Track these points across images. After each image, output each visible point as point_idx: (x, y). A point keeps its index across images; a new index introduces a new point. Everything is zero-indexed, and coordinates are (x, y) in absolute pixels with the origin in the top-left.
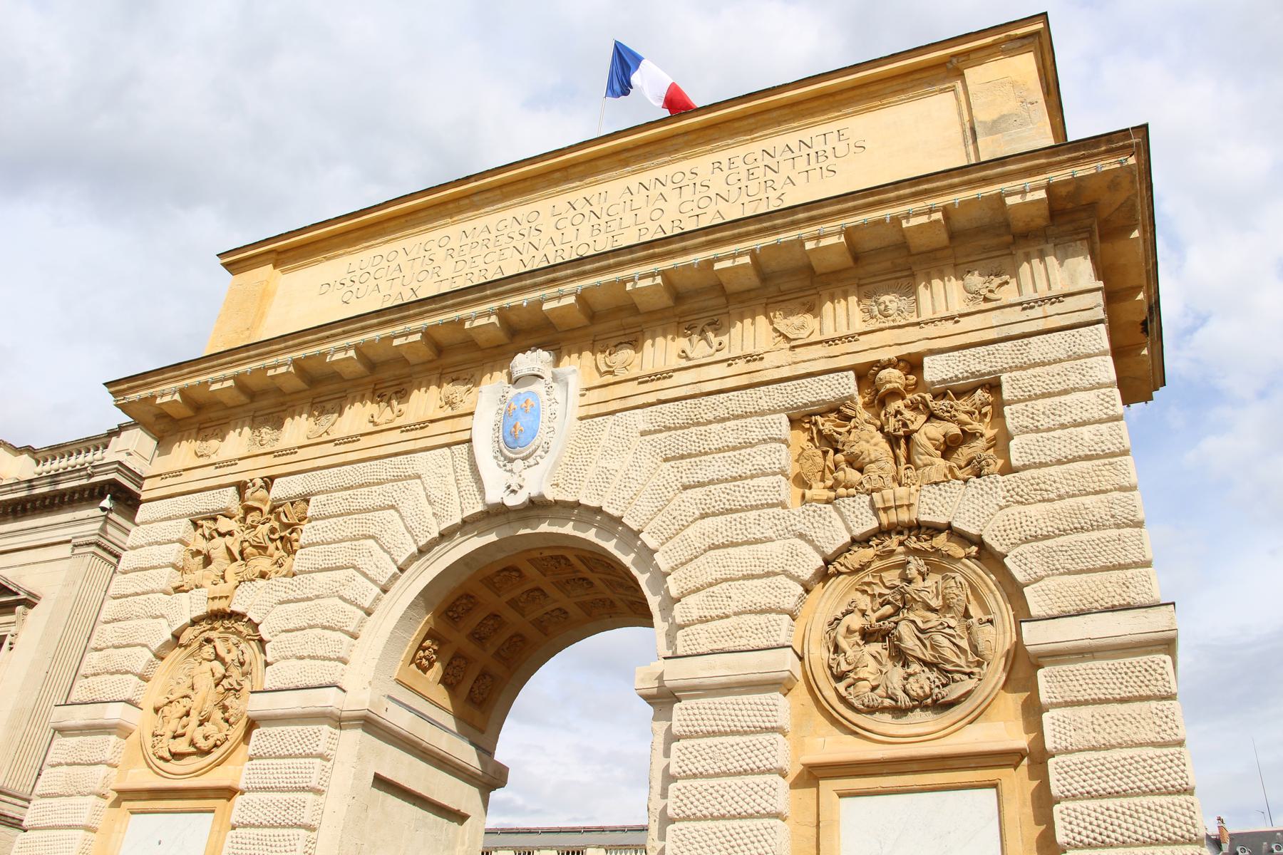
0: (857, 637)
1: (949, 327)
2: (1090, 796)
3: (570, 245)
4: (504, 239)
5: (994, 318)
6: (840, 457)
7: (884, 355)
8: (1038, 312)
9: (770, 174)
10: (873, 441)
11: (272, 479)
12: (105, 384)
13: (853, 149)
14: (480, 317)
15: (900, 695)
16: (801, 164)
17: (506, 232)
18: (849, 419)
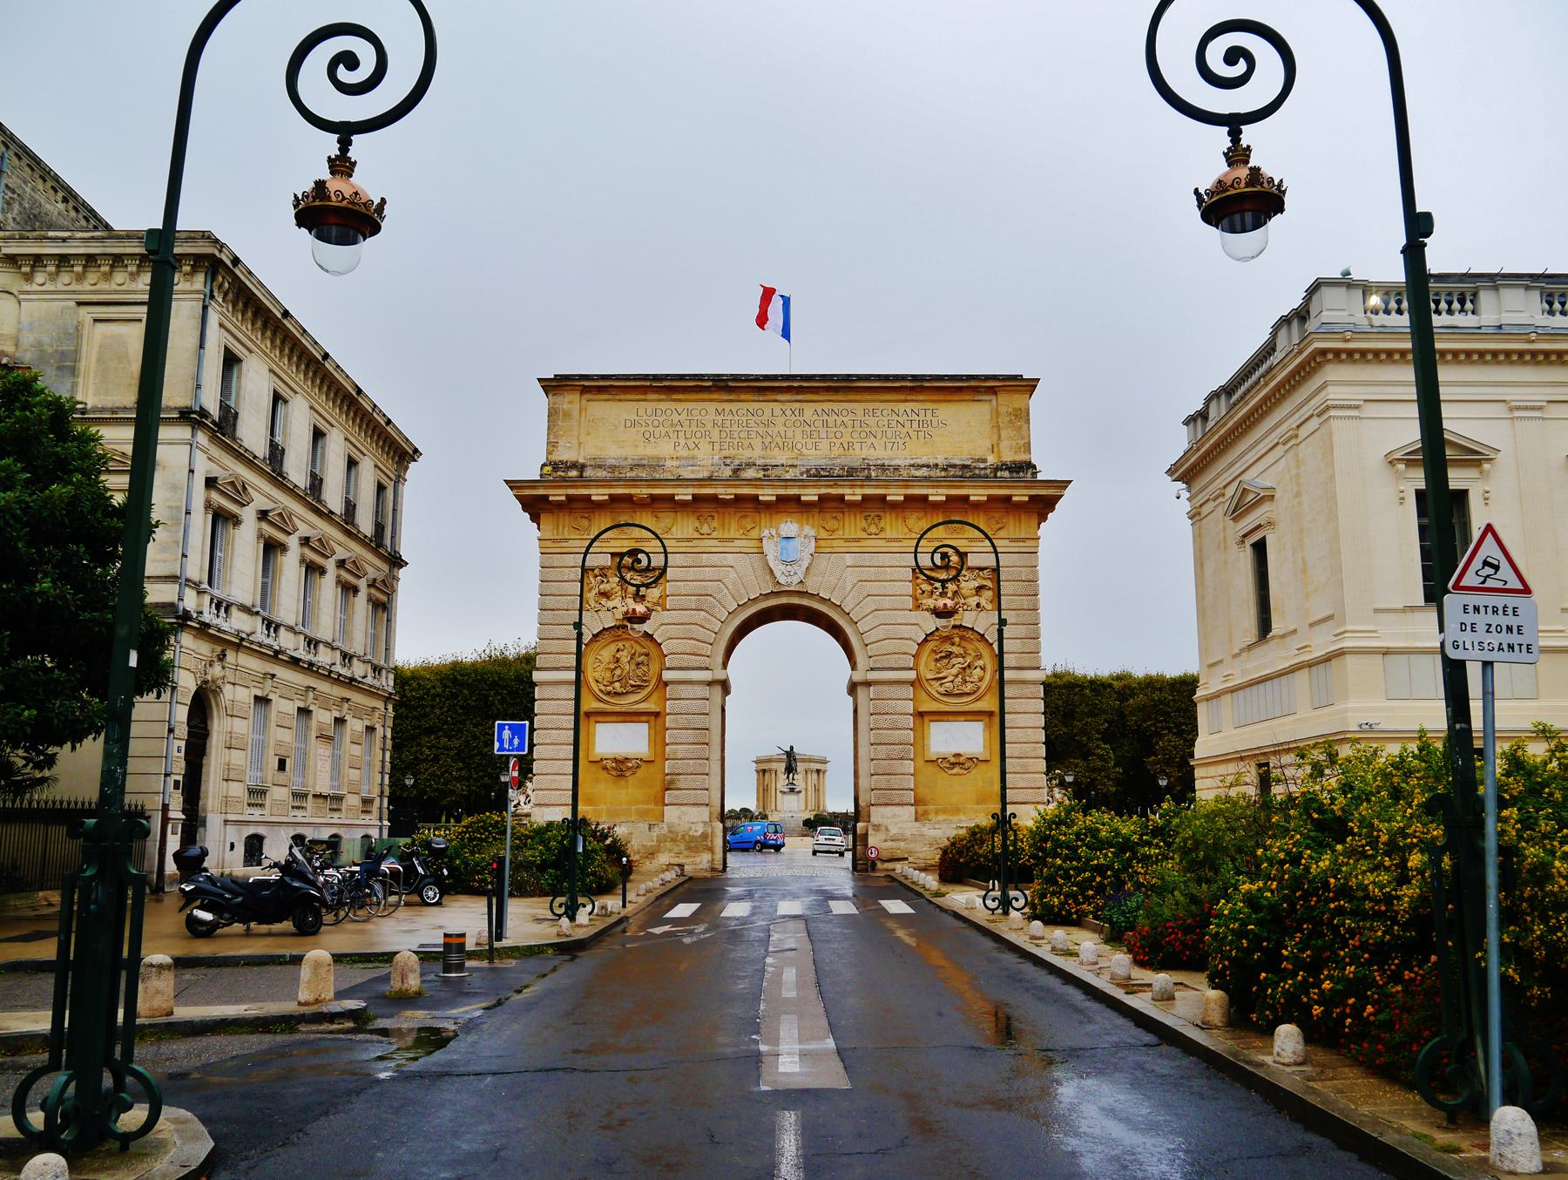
12: (512, 484)
14: (767, 494)
16: (915, 425)
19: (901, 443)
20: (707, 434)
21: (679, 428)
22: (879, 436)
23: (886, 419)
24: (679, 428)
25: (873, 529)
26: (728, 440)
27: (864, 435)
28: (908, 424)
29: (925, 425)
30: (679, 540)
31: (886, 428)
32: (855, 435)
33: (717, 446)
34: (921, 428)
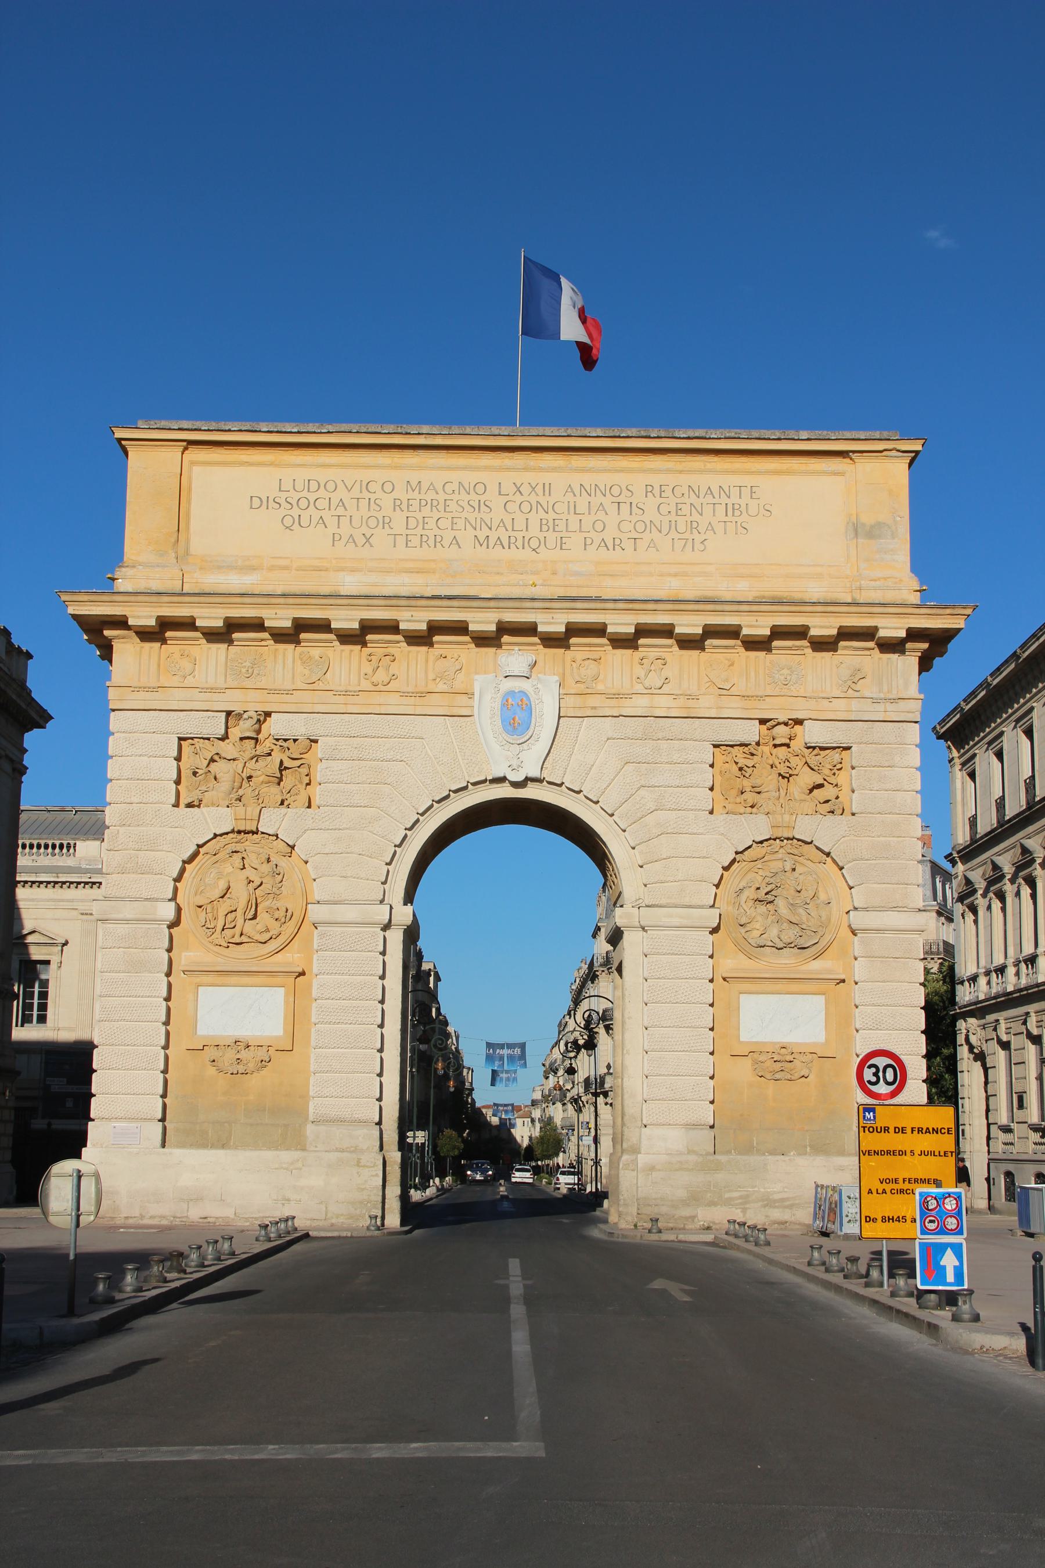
0: (751, 903)
1: (825, 702)
2: (874, 1005)
3: (522, 534)
4: (453, 506)
5: (855, 705)
6: (747, 784)
7: (783, 718)
8: (880, 707)
9: (696, 517)
10: (770, 777)
11: (268, 714)
13: (762, 511)
15: (777, 940)
17: (456, 497)
18: (752, 755)
19: (698, 538)
20: (386, 522)
21: (340, 511)
22: (665, 531)
23: (673, 501)
24: (340, 511)
25: (654, 680)
26: (419, 531)
27: (640, 527)
28: (708, 510)
29: (737, 513)
30: (337, 693)
31: (673, 517)
32: (626, 527)
33: (401, 541)
34: (730, 518)
